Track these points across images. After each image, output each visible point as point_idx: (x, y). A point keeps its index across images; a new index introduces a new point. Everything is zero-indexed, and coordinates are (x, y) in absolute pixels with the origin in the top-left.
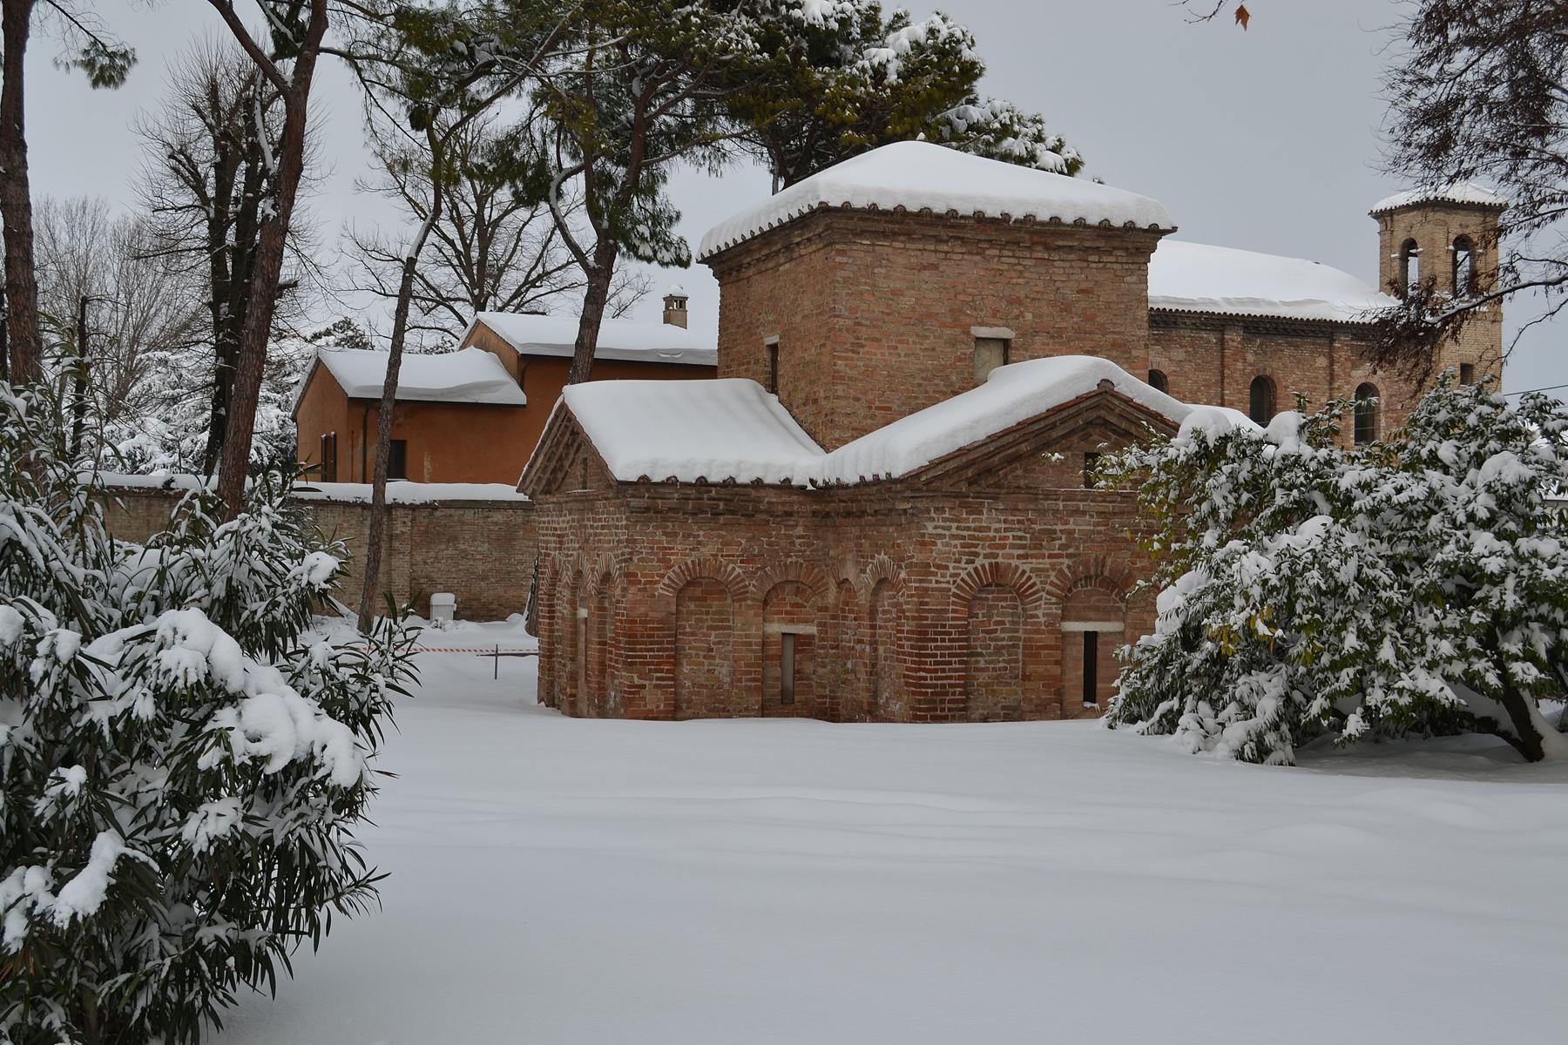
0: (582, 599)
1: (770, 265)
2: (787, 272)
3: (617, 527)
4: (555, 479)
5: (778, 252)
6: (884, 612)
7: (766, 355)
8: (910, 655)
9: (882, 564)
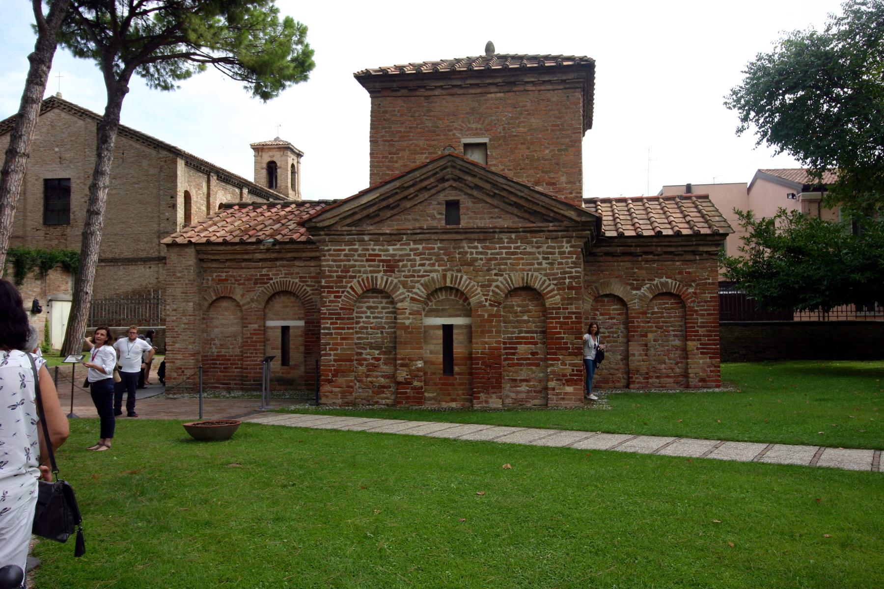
0: (431, 310)
1: (473, 91)
2: (497, 99)
3: (553, 253)
4: (378, 215)
5: (490, 84)
6: (653, 313)
7: (462, 149)
8: (704, 336)
9: (662, 284)
